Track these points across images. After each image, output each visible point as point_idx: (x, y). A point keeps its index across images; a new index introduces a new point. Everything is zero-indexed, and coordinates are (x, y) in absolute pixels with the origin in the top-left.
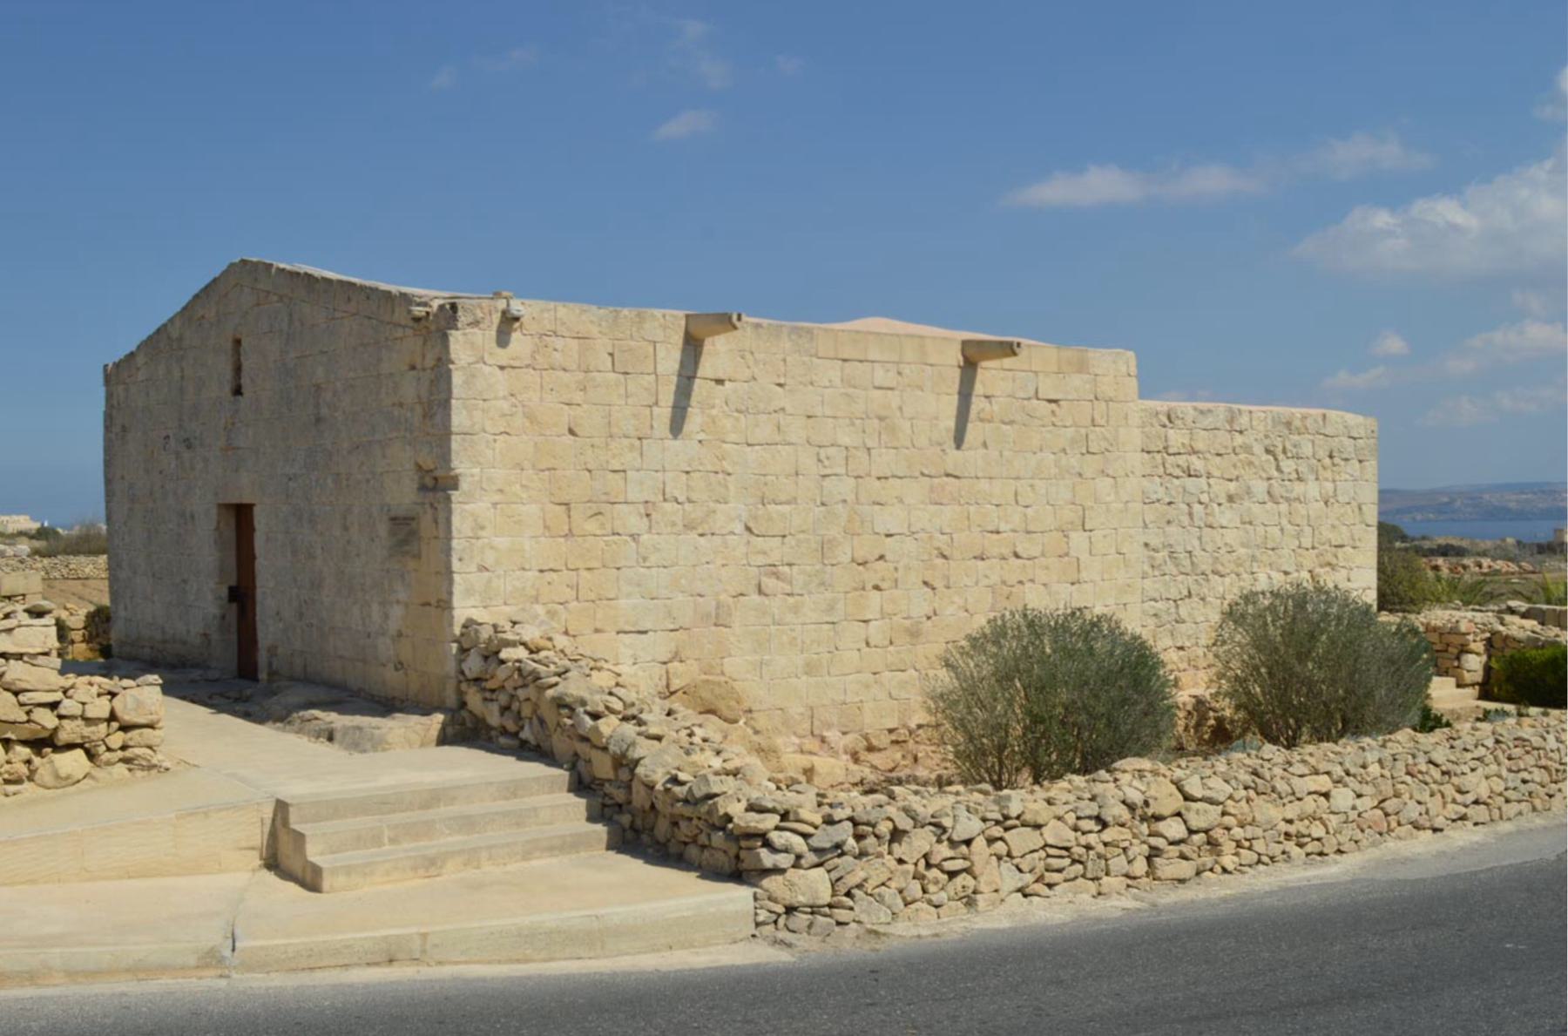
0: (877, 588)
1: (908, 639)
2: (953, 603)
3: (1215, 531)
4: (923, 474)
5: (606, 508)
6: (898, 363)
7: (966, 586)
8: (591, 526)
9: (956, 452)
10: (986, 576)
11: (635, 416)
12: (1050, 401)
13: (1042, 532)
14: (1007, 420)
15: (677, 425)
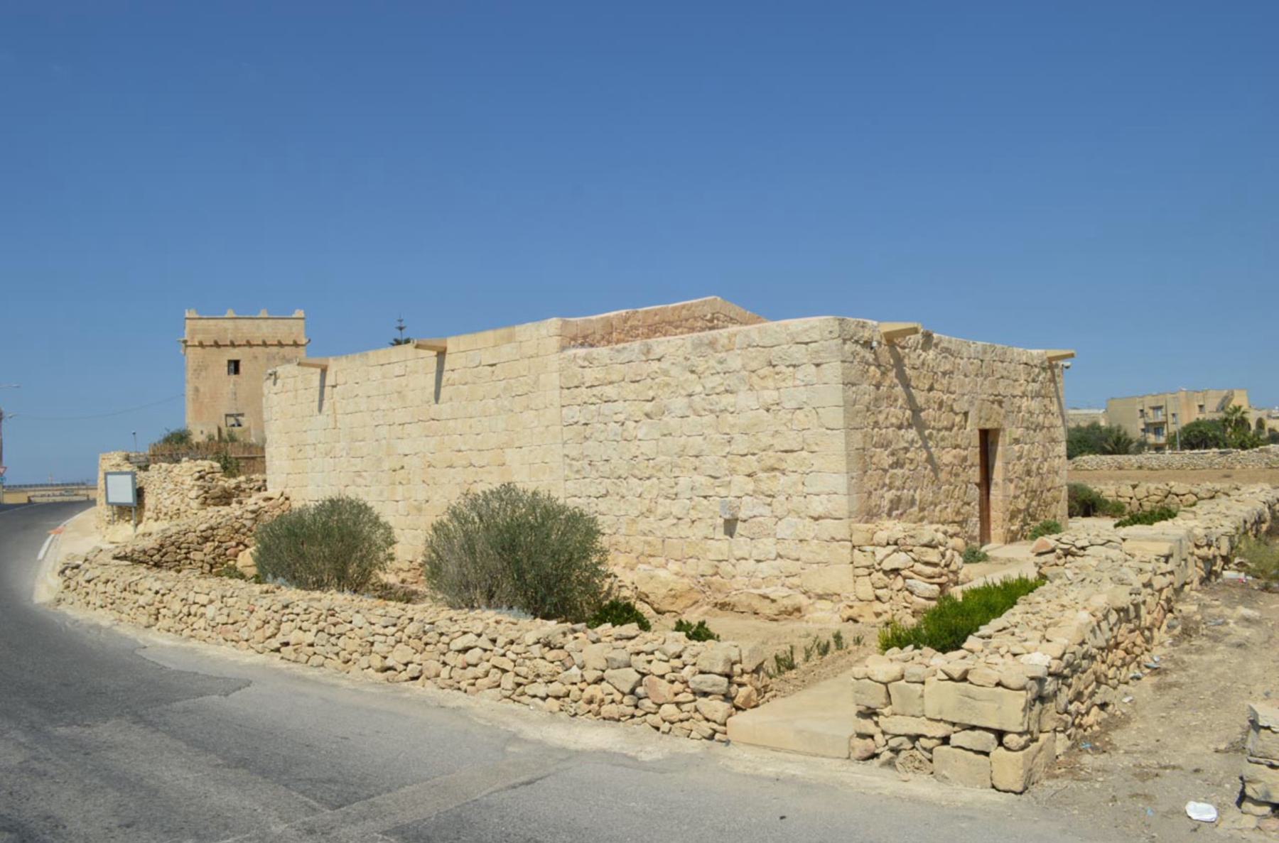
0: (400, 483)
3: (631, 443)
4: (420, 420)
5: (302, 447)
6: (405, 361)
8: (299, 455)
10: (454, 478)
15: (320, 409)
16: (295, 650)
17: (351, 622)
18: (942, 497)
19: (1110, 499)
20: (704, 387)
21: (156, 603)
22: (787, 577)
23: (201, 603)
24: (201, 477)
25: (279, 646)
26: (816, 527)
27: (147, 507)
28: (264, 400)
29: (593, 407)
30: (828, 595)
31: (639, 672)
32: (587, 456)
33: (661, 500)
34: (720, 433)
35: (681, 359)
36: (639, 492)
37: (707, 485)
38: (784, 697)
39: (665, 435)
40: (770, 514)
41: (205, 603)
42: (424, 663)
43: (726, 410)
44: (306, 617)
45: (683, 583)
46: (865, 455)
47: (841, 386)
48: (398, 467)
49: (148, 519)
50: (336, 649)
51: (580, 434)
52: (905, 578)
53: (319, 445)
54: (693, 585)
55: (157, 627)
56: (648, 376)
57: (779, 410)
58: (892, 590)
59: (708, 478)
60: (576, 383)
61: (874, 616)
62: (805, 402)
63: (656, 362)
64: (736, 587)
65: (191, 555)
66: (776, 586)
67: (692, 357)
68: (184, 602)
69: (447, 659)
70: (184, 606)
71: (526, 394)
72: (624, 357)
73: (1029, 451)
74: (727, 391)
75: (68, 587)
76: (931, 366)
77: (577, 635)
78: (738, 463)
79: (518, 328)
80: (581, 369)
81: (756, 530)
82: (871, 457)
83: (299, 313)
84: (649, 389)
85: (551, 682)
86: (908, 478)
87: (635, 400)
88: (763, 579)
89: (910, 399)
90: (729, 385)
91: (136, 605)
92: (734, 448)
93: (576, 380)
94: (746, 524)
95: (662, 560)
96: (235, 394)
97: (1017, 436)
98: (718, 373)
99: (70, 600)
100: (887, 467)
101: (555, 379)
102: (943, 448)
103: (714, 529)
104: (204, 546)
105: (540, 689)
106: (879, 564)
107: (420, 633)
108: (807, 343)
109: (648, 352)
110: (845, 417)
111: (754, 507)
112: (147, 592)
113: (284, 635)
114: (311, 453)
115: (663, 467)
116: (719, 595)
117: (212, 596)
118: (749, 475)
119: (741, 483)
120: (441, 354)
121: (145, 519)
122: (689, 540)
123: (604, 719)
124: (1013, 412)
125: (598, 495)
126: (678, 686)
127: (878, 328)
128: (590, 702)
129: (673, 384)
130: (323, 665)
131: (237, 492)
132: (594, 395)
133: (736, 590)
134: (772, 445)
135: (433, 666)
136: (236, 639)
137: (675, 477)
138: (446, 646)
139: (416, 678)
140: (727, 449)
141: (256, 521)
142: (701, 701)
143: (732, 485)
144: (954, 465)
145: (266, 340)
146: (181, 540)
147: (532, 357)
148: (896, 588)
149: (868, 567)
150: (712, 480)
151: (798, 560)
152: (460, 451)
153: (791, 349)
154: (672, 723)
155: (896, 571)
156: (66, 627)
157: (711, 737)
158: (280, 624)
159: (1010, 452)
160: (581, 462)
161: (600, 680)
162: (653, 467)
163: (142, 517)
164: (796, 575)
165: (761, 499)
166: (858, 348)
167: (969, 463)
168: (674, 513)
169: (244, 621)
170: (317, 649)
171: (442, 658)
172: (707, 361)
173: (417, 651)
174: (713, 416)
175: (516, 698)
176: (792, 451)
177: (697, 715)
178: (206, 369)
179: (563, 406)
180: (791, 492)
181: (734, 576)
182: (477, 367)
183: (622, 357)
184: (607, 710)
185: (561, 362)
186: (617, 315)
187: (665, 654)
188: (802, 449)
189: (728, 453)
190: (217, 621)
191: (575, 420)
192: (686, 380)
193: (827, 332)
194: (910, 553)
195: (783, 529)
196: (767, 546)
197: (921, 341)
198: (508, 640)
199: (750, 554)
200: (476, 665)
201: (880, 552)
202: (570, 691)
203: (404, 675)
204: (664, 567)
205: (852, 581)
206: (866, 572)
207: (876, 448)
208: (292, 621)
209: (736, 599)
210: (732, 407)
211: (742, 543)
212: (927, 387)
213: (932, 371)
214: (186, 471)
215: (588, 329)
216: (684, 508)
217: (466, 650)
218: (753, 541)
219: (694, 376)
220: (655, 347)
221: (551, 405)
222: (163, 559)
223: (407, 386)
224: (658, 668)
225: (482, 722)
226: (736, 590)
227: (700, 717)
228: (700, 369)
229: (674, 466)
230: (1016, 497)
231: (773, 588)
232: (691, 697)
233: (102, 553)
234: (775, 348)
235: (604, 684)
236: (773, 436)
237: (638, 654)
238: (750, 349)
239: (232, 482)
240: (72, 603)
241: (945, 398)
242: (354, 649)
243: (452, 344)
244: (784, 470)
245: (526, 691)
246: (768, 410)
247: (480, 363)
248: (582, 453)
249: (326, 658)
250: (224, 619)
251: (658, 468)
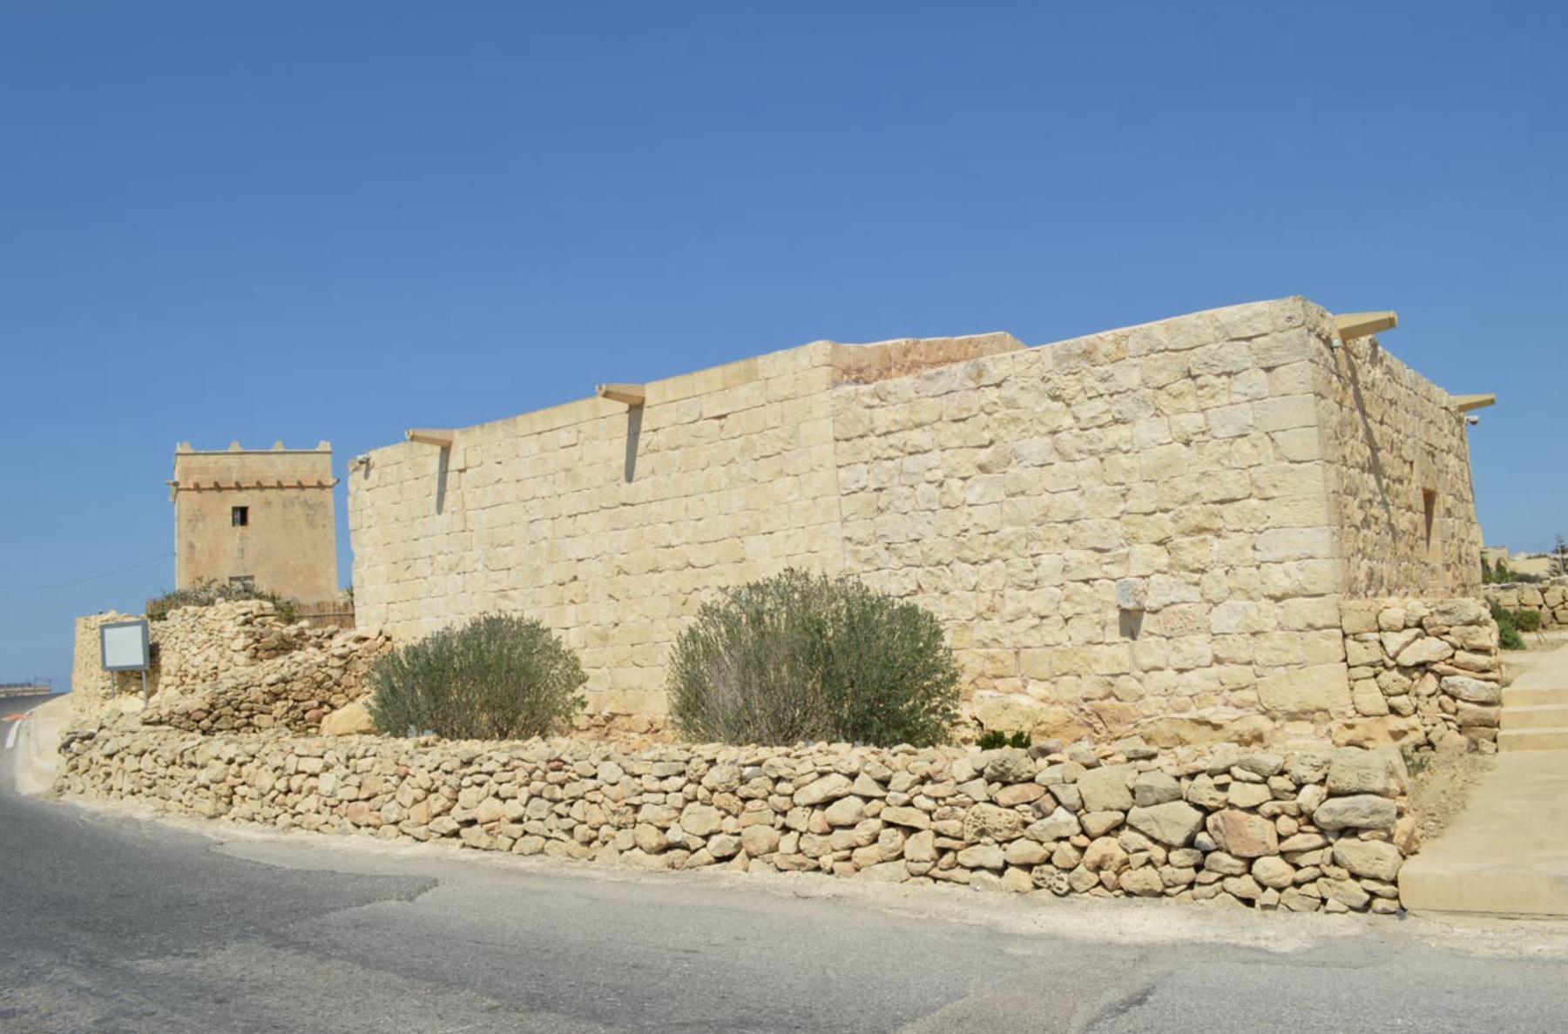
0: (572, 602)
1: (599, 642)
2: (633, 611)
5: (412, 562)
7: (644, 596)
8: (407, 575)
9: (627, 484)
10: (662, 587)
11: (422, 504)
12: (719, 417)
13: (715, 541)
14: (673, 446)
16: (488, 831)
17: (594, 777)
18: (1403, 578)
19: (1511, 610)
20: (1076, 418)
21: (230, 778)
22: (1232, 690)
23: (309, 771)
24: (246, 622)
25: (457, 826)
26: (1279, 611)
27: (164, 670)
28: (350, 500)
29: (889, 464)
30: (1305, 712)
31: (1198, 807)
32: (884, 536)
33: (1009, 592)
34: (1109, 485)
35: (1036, 380)
36: (974, 584)
37: (1089, 563)
38: (1436, 837)
39: (1013, 495)
40: (1199, 598)
41: (317, 771)
42: (744, 832)
43: (1116, 448)
44: (508, 776)
45: (1057, 713)
46: (1340, 502)
47: (1312, 395)
48: (567, 579)
49: (167, 686)
50: (567, 823)
51: (869, 505)
52: (1440, 676)
53: (440, 558)
54: (1072, 715)
55: (232, 815)
56: (982, 409)
57: (1208, 441)
58: (1417, 695)
59: (1090, 552)
60: (861, 431)
61: (1391, 740)
62: (1251, 426)
63: (994, 388)
64: (1147, 712)
65: (255, 721)
66: (1215, 705)
67: (1054, 376)
68: (278, 772)
69: (790, 821)
70: (278, 778)
71: (779, 454)
72: (941, 385)
74: (1116, 421)
75: (75, 768)
77: (1052, 757)
78: (1142, 526)
79: (760, 360)
80: (867, 411)
81: (1177, 623)
82: (1345, 506)
83: (324, 446)
84: (984, 429)
85: (1010, 841)
86: (1376, 545)
87: (961, 447)
88: (1191, 696)
89: (1369, 432)
90: (1120, 413)
91: (195, 784)
92: (1133, 504)
93: (860, 426)
94: (1158, 616)
95: (1018, 682)
96: (242, 550)
97: (1448, 506)
98: (1101, 395)
99: (80, 787)
100: (1359, 524)
101: (827, 429)
102: (1399, 508)
103: (1103, 628)
104: (273, 706)
105: (995, 857)
106: (1393, 659)
107: (735, 783)
108: (1248, 339)
109: (980, 375)
110: (1319, 443)
111: (1171, 589)
112: (212, 762)
113: (464, 808)
114: (426, 570)
115: (1012, 542)
116: (1118, 727)
117: (330, 758)
118: (1160, 543)
119: (1146, 555)
120: (636, 409)
121: (161, 687)
122: (1060, 648)
123: (1129, 894)
125: (903, 593)
126: (1286, 824)
127: (1336, 323)
128: (1098, 868)
129: (1023, 418)
130: (542, 851)
131: (300, 642)
132: (891, 446)
133: (1146, 717)
134: (1198, 494)
135: (761, 834)
136: (377, 822)
137: (1033, 556)
138: (788, 799)
139: (730, 858)
140: (1122, 507)
141: (346, 670)
142: (1343, 846)
143: (1132, 560)
144: (1410, 534)
145: (282, 480)
146: (240, 698)
147: (787, 399)
148: (1424, 691)
149: (1372, 665)
150: (1097, 555)
151: (1249, 663)
152: (668, 547)
153: (1222, 350)
154: (1280, 889)
155: (1423, 667)
156: (82, 821)
157: (1367, 907)
158: (459, 791)
160: (872, 547)
161: (1115, 829)
162: (995, 544)
163: (156, 685)
164: (1247, 686)
165: (1183, 577)
166: (1321, 344)
167: (1418, 534)
168: (1034, 610)
169: (387, 793)
170: (528, 826)
171: (780, 820)
172: (1078, 380)
173: (729, 813)
174: (1095, 459)
175: (940, 874)
176: (1232, 500)
177: (1333, 871)
178: (204, 519)
179: (840, 467)
180: (1233, 561)
181: (1141, 697)
182: (694, 422)
183: (934, 389)
184: (1130, 880)
185: (834, 402)
186: (896, 344)
187: (1254, 770)
188: (1250, 496)
189: (1122, 512)
190: (339, 797)
191: (861, 484)
192: (1048, 410)
193: (1282, 320)
194: (1443, 637)
195: (1222, 619)
196: (1199, 646)
197: (1369, 352)
198: (917, 777)
199: (1167, 661)
200: (852, 826)
201: (1393, 641)
202: (1052, 853)
203: (705, 855)
204: (1020, 692)
205: (1348, 687)
206: (1370, 672)
207: (1347, 495)
208: (480, 785)
209: (1152, 728)
210: (1126, 442)
211: (1153, 645)
212: (1379, 418)
213: (1381, 397)
214: (226, 614)
215: (863, 360)
216: (1052, 600)
217: (827, 803)
218: (1171, 641)
219: (1058, 405)
220: (990, 364)
221: (821, 466)
222: (215, 725)
223: (580, 459)
224: (1242, 794)
225: (905, 914)
226: (1146, 717)
227: (1344, 873)
228: (1069, 393)
229: (1033, 538)
230: (1453, 591)
231: (1213, 709)
232: (1318, 840)
233: (123, 718)
234: (1195, 350)
235: (1126, 834)
236: (1198, 481)
237: (1192, 776)
238: (1153, 356)
239: (292, 629)
240: (82, 792)
242: (603, 819)
243: (652, 392)
244: (1220, 529)
245: (960, 859)
246: (1187, 443)
247: (701, 415)
248: (874, 533)
249: (548, 838)
250: (352, 792)
251: (1003, 544)
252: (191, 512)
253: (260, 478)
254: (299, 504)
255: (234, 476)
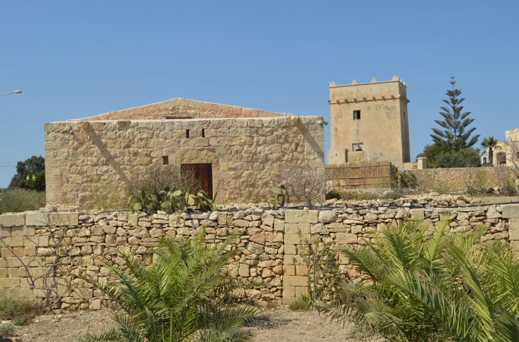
73: (250, 175)
76: (127, 137)
96: (358, 131)
97: (233, 166)
124: (231, 154)
159: (224, 174)
178: (341, 117)
197: (118, 126)
241: (140, 151)
252: (336, 114)
253: (365, 97)
254: (383, 107)
255: (354, 96)
